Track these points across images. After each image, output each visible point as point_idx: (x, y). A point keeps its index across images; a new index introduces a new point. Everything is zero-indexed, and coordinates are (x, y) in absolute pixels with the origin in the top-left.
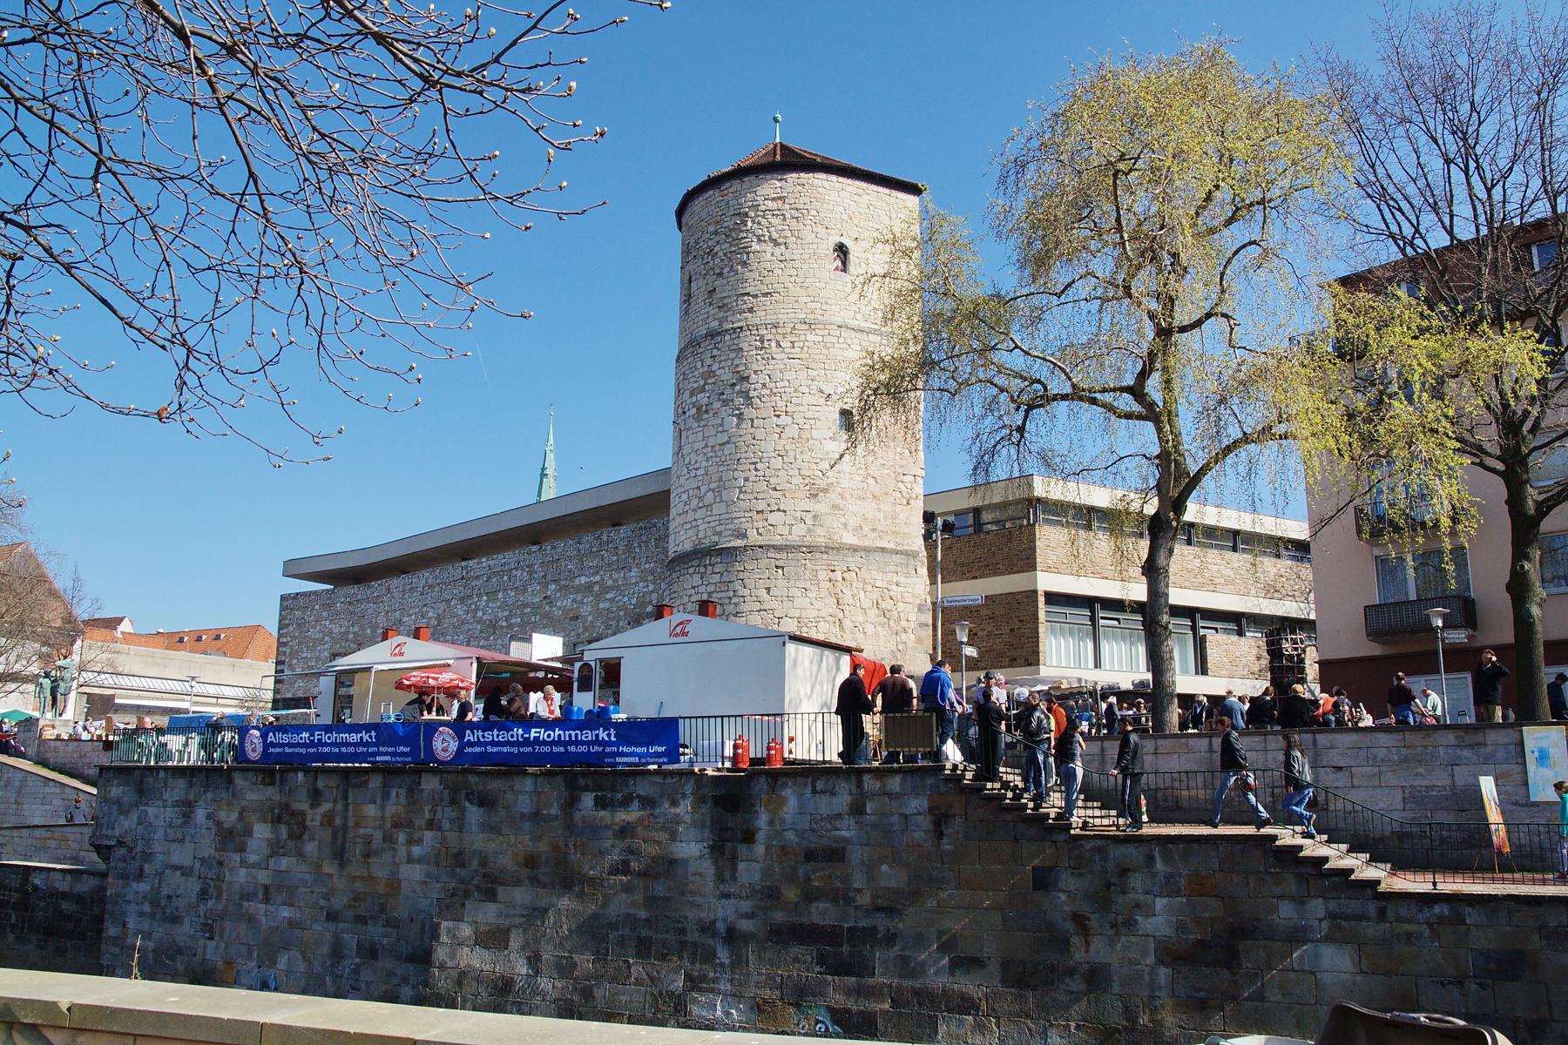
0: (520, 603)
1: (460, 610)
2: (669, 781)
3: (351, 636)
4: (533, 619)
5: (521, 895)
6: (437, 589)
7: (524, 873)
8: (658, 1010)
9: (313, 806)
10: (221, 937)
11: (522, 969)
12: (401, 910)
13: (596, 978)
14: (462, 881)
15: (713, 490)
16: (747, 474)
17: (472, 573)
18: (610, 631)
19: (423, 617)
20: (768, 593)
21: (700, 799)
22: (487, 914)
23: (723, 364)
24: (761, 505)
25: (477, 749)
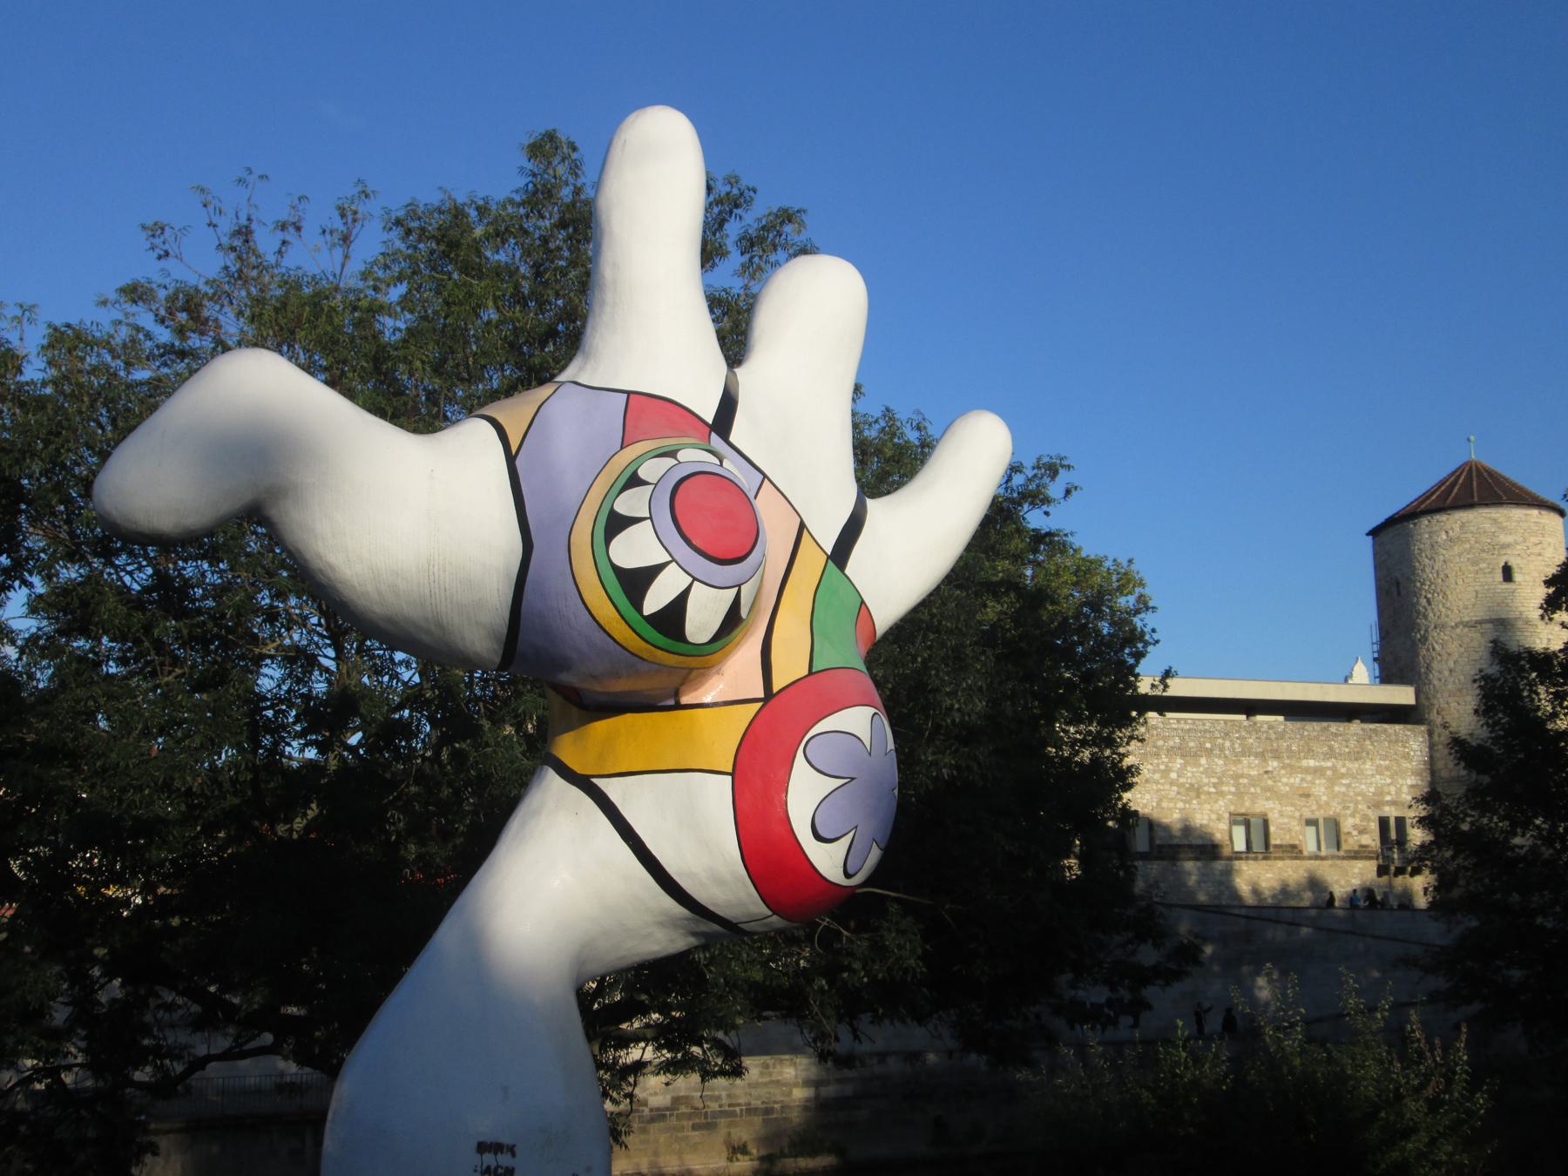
18: (1349, 812)
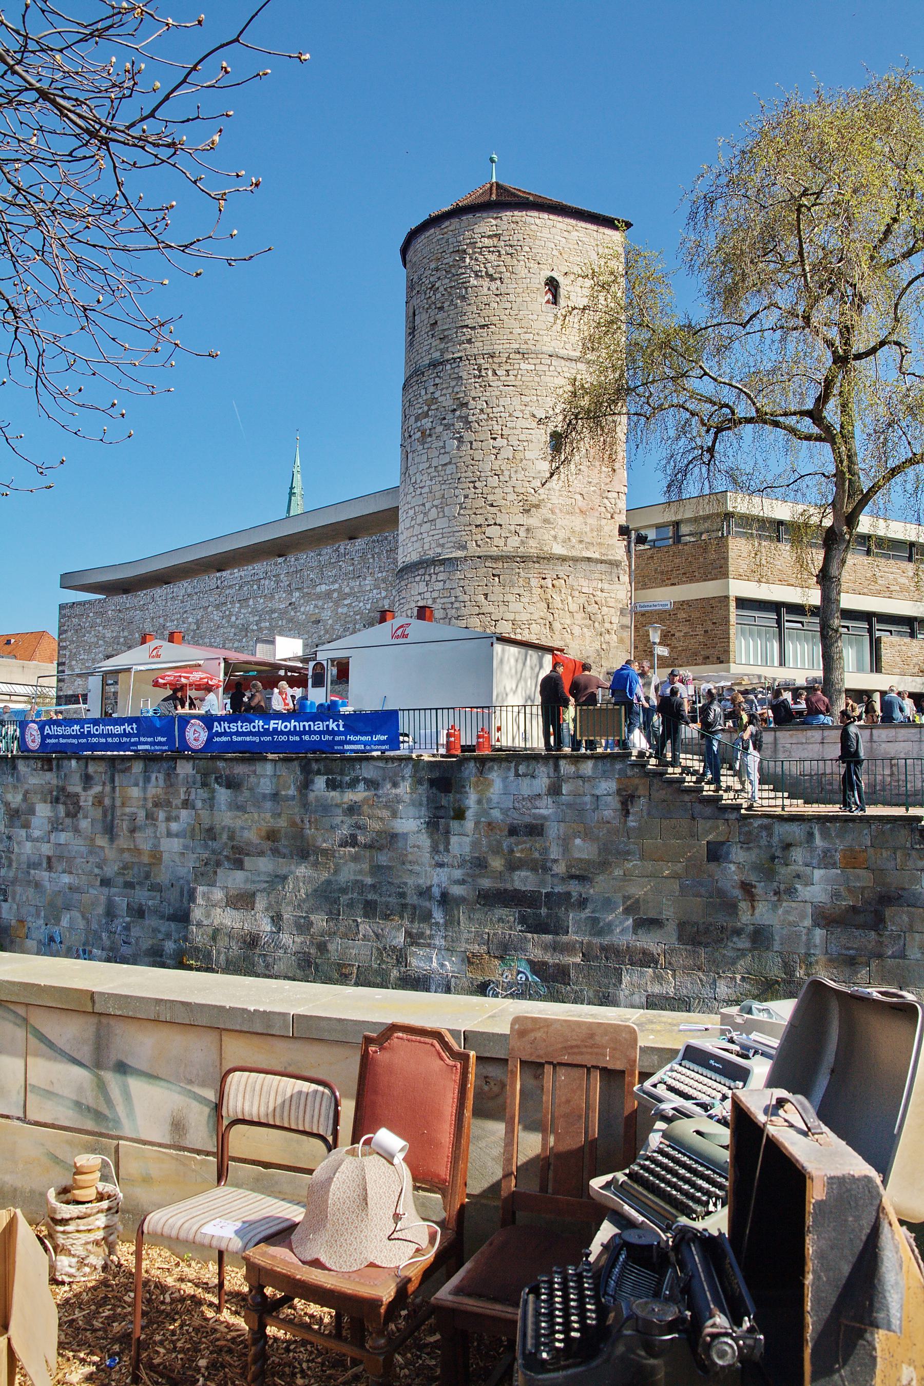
0: (268, 609)
1: (216, 615)
2: (390, 765)
3: (122, 640)
4: (280, 623)
5: (264, 865)
6: (195, 597)
7: (267, 845)
8: (383, 961)
9: (85, 789)
10: (14, 899)
11: (266, 926)
12: (163, 877)
13: (329, 935)
14: (214, 852)
15: (436, 507)
16: (467, 492)
17: (226, 583)
19: (184, 622)
20: (486, 598)
21: (418, 782)
22: (236, 880)
23: (444, 392)
24: (480, 520)
25: (224, 739)
